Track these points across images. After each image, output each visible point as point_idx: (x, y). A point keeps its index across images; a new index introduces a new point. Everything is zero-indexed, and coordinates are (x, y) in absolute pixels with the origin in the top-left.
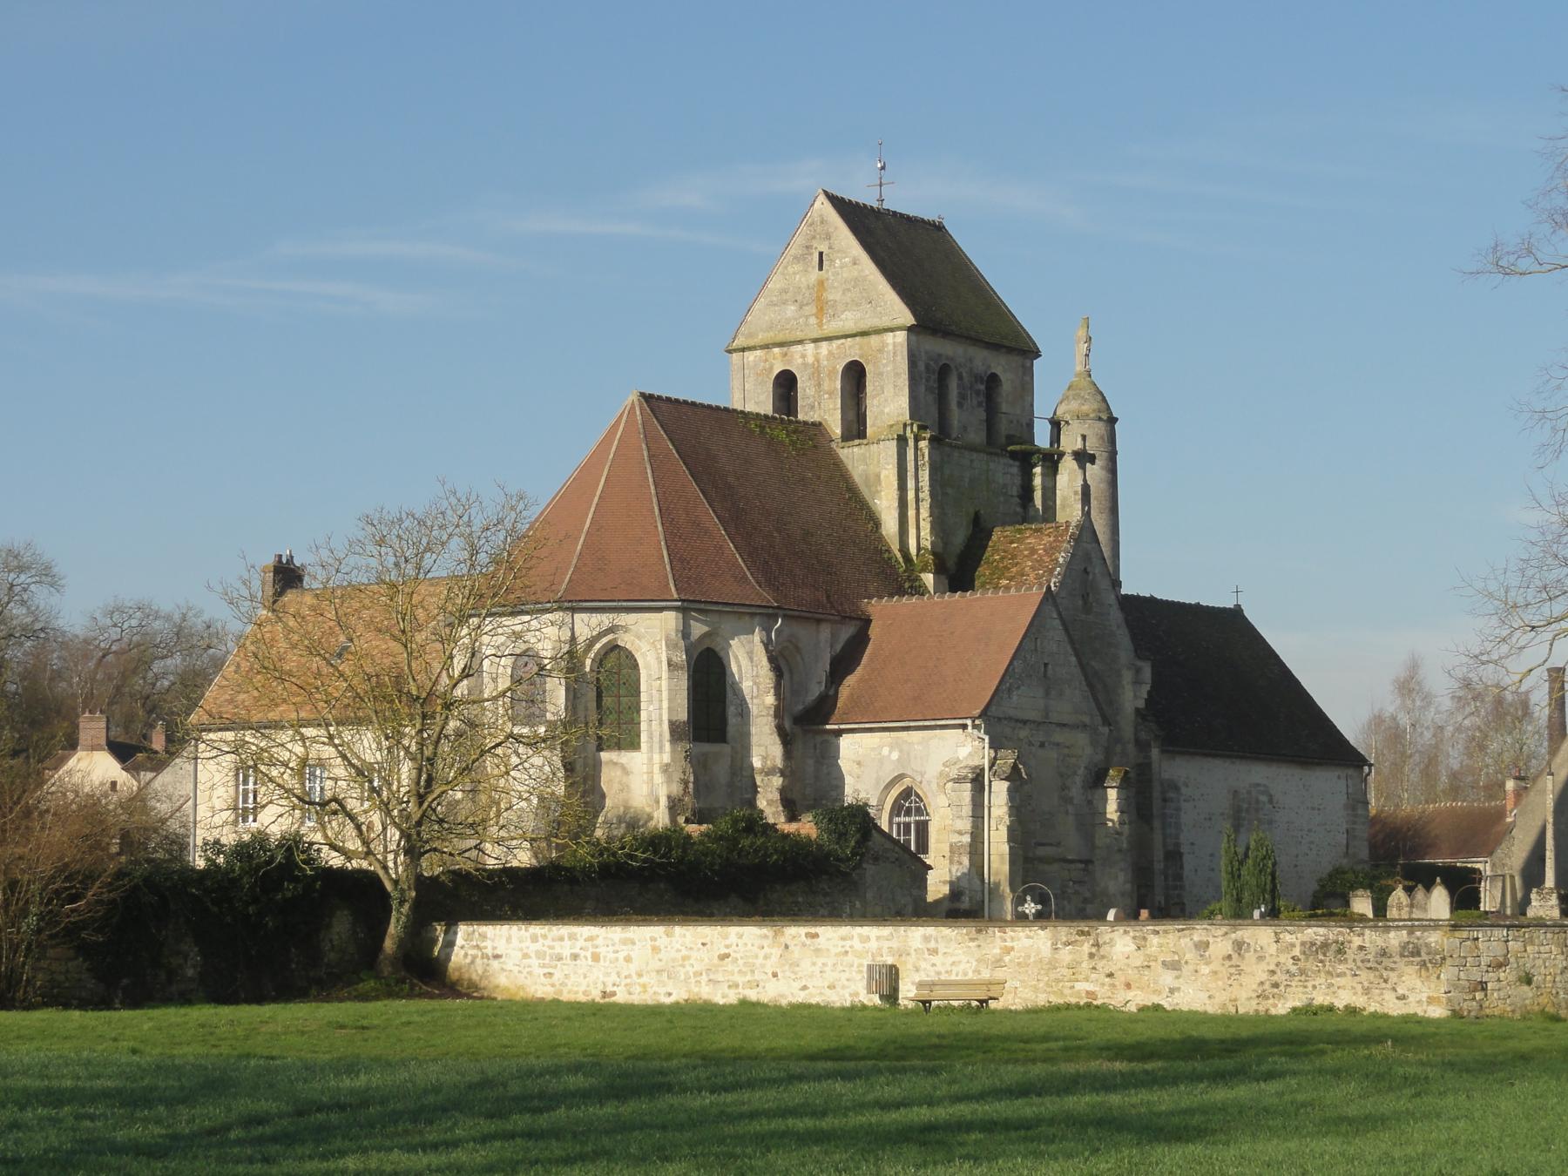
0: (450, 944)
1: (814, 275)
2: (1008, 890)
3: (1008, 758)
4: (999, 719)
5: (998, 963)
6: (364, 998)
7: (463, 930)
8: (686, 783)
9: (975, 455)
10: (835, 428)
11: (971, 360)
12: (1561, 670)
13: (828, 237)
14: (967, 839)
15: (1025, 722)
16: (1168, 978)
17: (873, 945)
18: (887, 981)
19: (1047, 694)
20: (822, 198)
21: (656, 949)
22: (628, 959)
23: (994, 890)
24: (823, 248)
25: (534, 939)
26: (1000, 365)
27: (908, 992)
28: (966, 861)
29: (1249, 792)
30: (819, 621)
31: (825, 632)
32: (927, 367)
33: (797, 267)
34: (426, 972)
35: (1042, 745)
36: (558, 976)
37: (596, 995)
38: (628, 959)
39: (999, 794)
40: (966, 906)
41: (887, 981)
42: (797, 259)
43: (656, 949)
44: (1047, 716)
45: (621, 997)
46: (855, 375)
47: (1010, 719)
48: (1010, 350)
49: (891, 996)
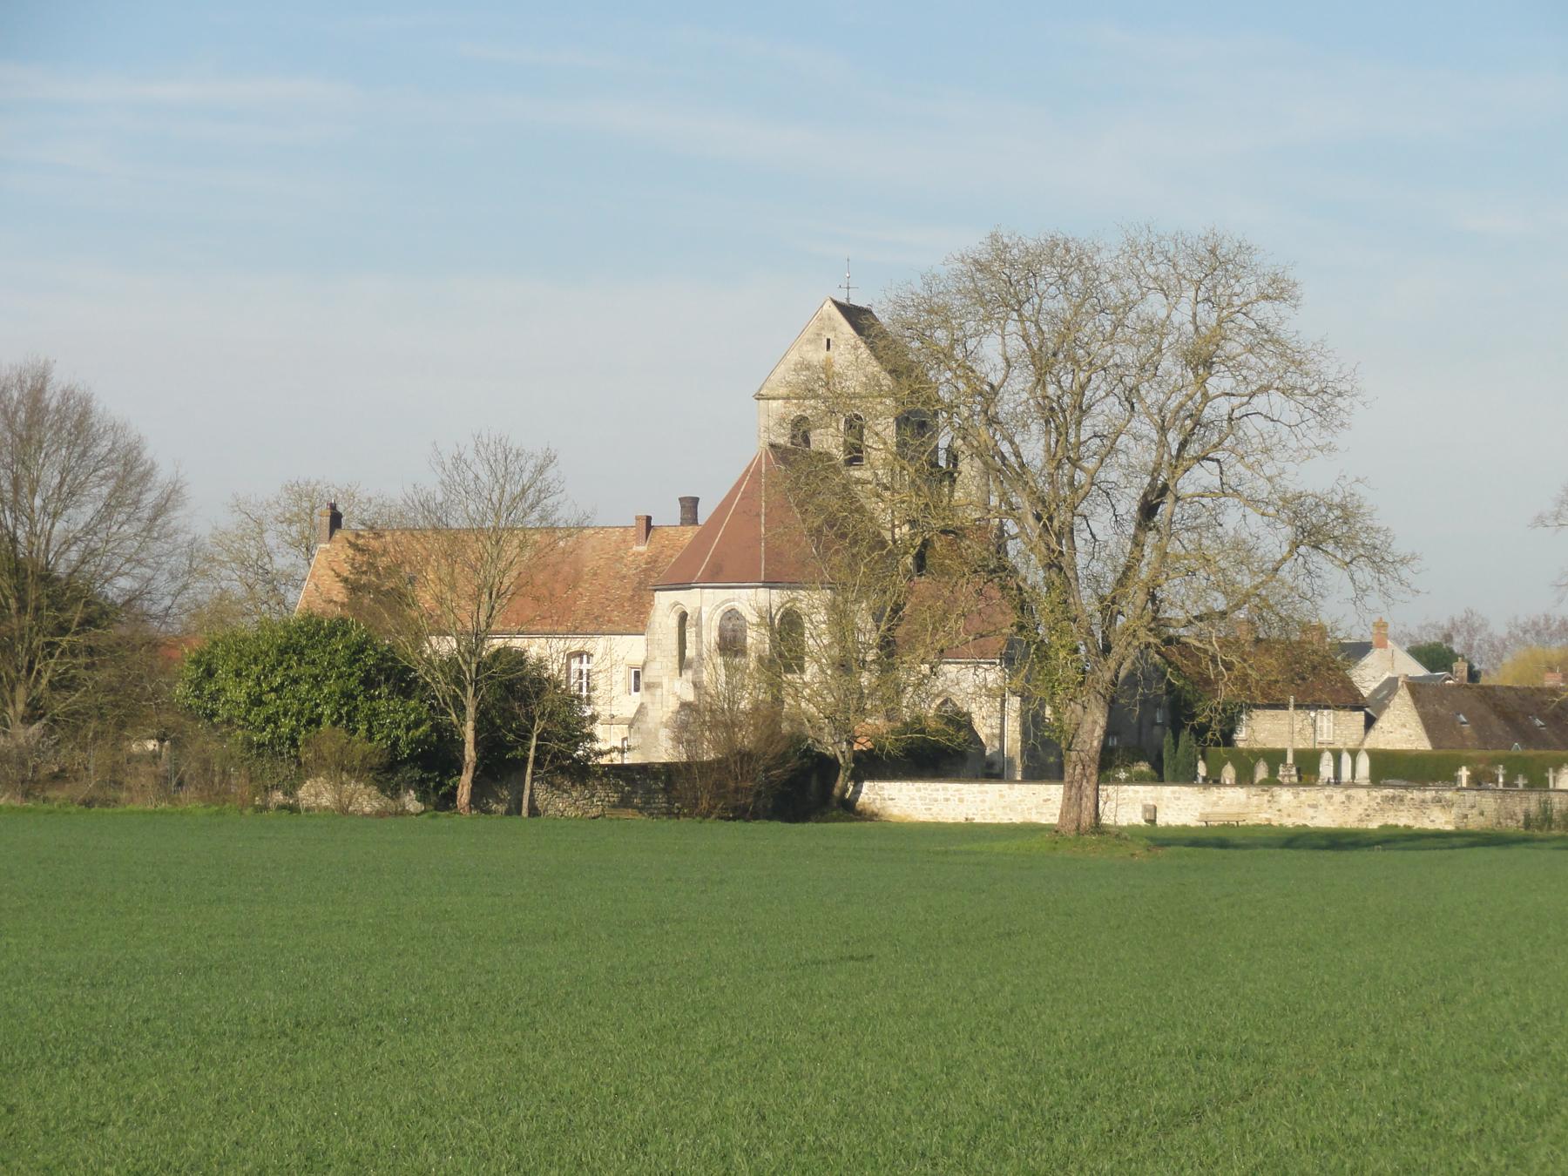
0: (857, 792)
1: (823, 354)
2: (1018, 761)
3: (1018, 682)
5: (1216, 804)
6: (835, 820)
7: (866, 785)
10: (840, 456)
12: (695, 501)
13: (834, 329)
14: (997, 731)
16: (1311, 812)
17: (1141, 795)
18: (1151, 812)
20: (829, 303)
21: (1002, 796)
22: (983, 801)
23: (1011, 761)
24: (831, 336)
25: (919, 790)
27: (1161, 821)
28: (997, 744)
33: (809, 347)
34: (849, 809)
36: (935, 809)
37: (962, 820)
38: (983, 801)
39: (1014, 703)
40: (992, 771)
41: (1151, 812)
42: (809, 341)
43: (1002, 796)
45: (978, 820)
46: (855, 426)
49: (1153, 822)
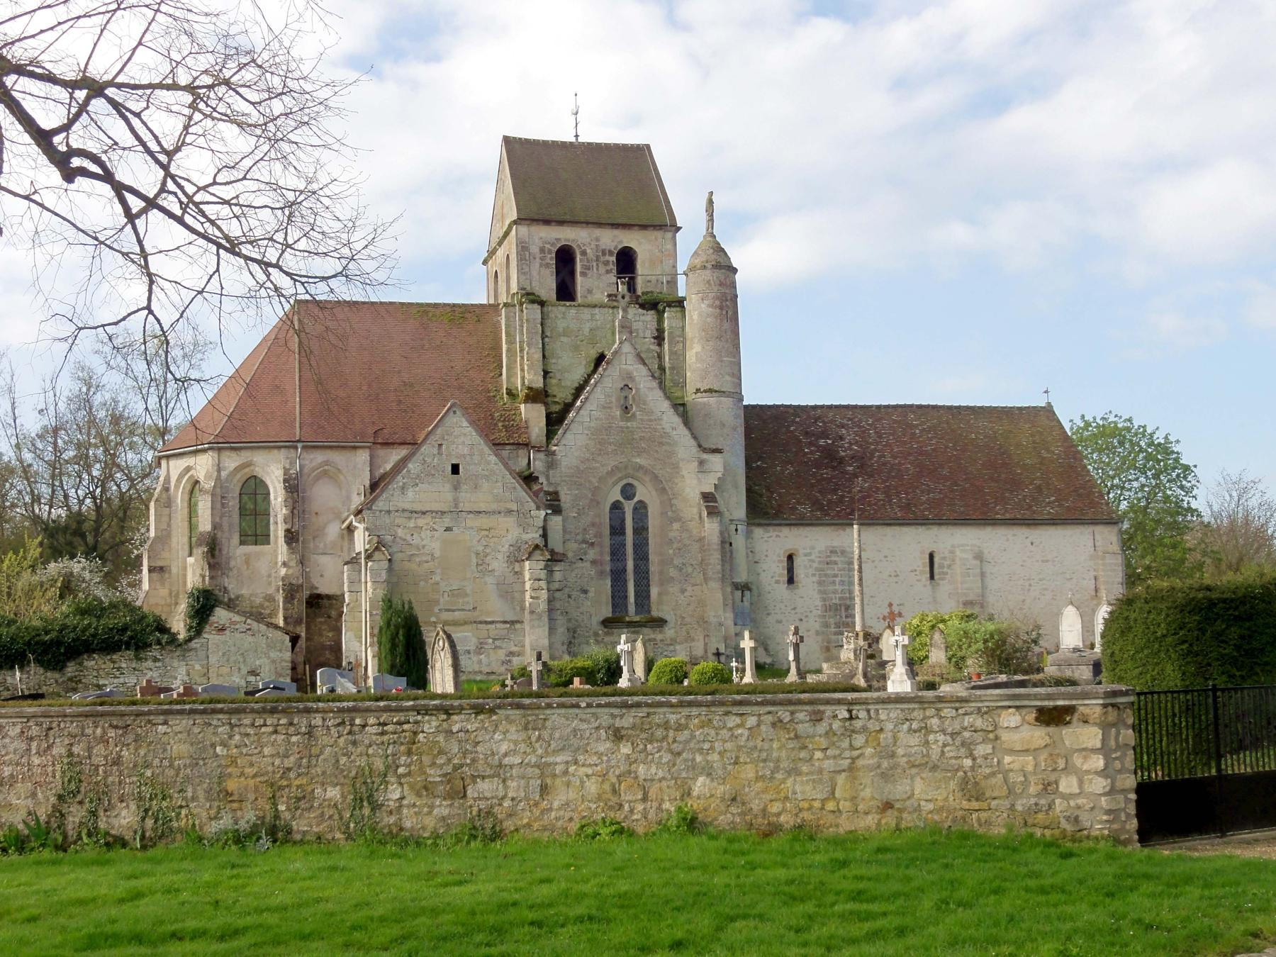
4: (389, 512)
8: (203, 577)
9: (597, 310)
11: (597, 239)
15: (424, 513)
19: (456, 488)
26: (636, 241)
29: (952, 552)
30: (355, 448)
31: (363, 457)
32: (542, 250)
35: (448, 529)
44: (456, 506)
47: (404, 510)
48: (644, 227)
